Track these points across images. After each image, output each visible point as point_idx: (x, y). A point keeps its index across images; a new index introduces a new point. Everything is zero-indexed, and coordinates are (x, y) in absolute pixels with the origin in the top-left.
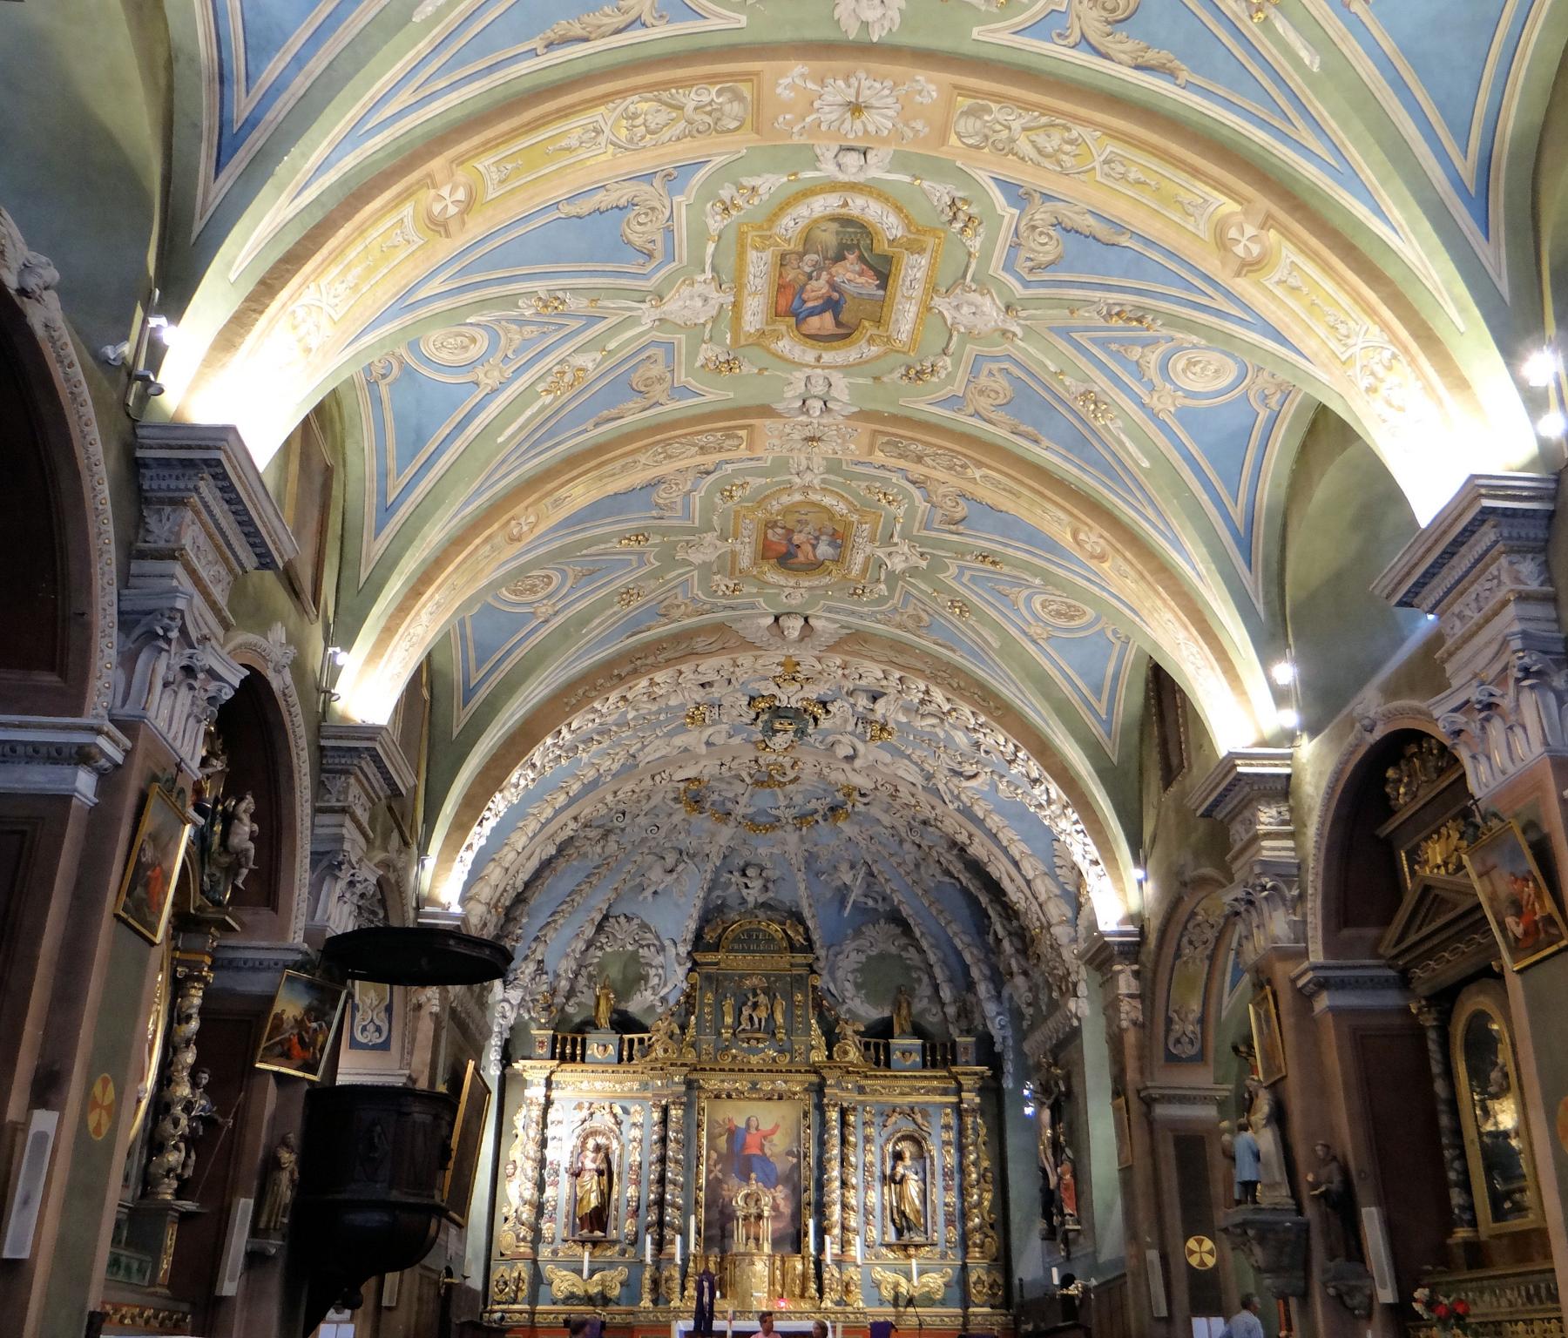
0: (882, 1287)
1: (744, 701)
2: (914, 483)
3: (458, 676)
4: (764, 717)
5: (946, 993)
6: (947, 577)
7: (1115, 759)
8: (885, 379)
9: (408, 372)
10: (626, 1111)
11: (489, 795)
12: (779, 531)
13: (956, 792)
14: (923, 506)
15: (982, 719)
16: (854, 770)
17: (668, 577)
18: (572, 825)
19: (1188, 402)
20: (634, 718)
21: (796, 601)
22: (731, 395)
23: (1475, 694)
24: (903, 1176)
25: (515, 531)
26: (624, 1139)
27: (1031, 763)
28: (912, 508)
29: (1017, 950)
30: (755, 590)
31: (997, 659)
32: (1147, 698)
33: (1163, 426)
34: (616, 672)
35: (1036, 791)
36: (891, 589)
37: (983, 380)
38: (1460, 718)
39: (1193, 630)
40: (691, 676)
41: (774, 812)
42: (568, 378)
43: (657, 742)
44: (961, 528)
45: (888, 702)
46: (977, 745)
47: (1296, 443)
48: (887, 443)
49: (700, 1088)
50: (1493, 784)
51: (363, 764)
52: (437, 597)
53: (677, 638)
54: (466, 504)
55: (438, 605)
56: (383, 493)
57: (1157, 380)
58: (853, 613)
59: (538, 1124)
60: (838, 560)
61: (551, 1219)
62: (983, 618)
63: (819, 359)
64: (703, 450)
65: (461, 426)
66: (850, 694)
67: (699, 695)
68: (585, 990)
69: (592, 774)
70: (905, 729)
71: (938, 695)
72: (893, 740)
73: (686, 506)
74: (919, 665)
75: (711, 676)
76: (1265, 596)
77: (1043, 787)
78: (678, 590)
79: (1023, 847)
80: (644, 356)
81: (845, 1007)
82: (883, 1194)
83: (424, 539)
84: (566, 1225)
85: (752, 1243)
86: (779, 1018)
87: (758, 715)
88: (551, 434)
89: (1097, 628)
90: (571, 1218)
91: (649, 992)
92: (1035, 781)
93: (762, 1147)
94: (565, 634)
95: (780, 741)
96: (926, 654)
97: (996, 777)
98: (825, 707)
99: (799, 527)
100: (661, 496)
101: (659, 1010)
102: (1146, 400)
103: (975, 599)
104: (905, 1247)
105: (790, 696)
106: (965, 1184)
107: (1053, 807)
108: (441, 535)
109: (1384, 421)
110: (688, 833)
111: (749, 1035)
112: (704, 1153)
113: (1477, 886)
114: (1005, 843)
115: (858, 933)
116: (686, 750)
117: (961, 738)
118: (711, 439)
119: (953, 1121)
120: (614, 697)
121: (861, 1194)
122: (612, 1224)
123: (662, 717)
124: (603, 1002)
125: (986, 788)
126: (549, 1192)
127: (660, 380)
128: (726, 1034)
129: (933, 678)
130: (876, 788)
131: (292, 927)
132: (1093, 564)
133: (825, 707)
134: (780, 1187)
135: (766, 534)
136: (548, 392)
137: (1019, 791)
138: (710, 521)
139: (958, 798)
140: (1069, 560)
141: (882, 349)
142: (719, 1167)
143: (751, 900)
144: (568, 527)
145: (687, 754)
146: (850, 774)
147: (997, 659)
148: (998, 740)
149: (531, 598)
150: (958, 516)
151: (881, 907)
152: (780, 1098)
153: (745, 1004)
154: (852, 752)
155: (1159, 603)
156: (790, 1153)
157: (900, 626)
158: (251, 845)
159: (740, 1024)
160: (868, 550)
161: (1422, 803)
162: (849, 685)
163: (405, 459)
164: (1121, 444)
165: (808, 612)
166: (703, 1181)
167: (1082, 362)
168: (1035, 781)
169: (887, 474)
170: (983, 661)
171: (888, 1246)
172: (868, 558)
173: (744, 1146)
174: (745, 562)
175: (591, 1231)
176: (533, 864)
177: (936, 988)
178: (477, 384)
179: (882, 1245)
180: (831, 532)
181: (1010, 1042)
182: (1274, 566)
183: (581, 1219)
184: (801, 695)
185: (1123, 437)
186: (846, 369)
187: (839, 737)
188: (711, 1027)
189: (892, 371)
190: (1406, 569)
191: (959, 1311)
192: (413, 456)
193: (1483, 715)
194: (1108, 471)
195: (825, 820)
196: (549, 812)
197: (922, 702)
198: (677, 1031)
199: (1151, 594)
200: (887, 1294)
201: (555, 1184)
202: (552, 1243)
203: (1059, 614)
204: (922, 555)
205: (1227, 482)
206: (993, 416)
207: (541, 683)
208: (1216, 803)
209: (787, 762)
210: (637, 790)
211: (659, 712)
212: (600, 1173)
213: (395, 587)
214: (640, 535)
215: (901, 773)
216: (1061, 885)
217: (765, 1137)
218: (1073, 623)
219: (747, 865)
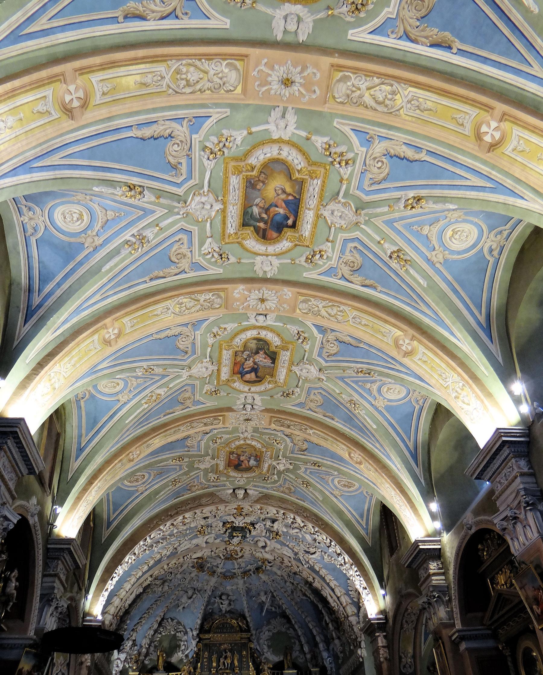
1: (221, 524)
2: (287, 436)
3: (105, 516)
4: (230, 531)
5: (306, 649)
6: (301, 472)
7: (370, 544)
8: (275, 397)
9: (92, 396)
11: (116, 567)
12: (235, 455)
13: (307, 560)
14: (290, 445)
15: (317, 529)
16: (266, 552)
17: (191, 474)
18: (150, 579)
19: (389, 403)
20: (176, 533)
21: (241, 483)
22: (216, 404)
23: (508, 513)
25: (131, 457)
27: (337, 547)
28: (286, 446)
29: (335, 628)
30: (225, 479)
31: (322, 505)
32: (381, 519)
33: (380, 412)
34: (169, 513)
35: (340, 559)
36: (279, 478)
37: (312, 397)
38: (505, 523)
39: (397, 491)
40: (200, 514)
41: (233, 571)
42: (154, 398)
43: (186, 542)
44: (305, 453)
45: (279, 523)
46: (315, 540)
47: (430, 417)
50: (521, 550)
51: (65, 555)
52: (99, 484)
53: (194, 499)
54: (112, 447)
55: (99, 488)
56: (79, 443)
57: (377, 395)
58: (264, 487)
60: (258, 466)
62: (315, 488)
63: (250, 389)
64: (205, 424)
65: (112, 417)
66: (263, 520)
67: (203, 522)
68: (153, 652)
69: (158, 556)
70: (286, 534)
71: (299, 520)
72: (281, 539)
73: (199, 446)
74: (291, 508)
75: (208, 514)
76: (424, 475)
77: (342, 557)
78: (195, 480)
79: (335, 582)
80: (183, 389)
81: (264, 657)
83: (95, 461)
87: (226, 530)
88: (147, 419)
89: (360, 491)
91: (181, 652)
92: (339, 555)
94: (149, 498)
95: (236, 540)
96: (293, 503)
97: (323, 553)
98: (253, 526)
99: (243, 454)
100: (189, 443)
101: (185, 661)
102: (373, 403)
103: (312, 480)
105: (239, 522)
107: (347, 565)
108: (102, 460)
109: (463, 409)
110: (198, 581)
111: (223, 671)
113: (520, 593)
114: (328, 581)
115: (269, 623)
116: (197, 545)
117: (308, 538)
118: (209, 420)
120: (168, 524)
123: (188, 532)
124: (160, 658)
125: (319, 558)
127: (189, 398)
129: (297, 513)
130: (275, 559)
131: (30, 628)
132: (357, 466)
133: (253, 526)
135: (230, 457)
136: (146, 403)
137: (333, 559)
138: (208, 452)
139: (308, 562)
141: (274, 385)
143: (224, 609)
145: (197, 547)
146: (264, 554)
147: (322, 505)
148: (323, 537)
149: (137, 484)
150: (304, 448)
153: (221, 657)
154: (264, 544)
155: (384, 480)
157: (282, 492)
158: (15, 592)
160: (270, 462)
161: (493, 559)
162: (263, 517)
163: (89, 430)
164: (365, 419)
167: (349, 390)
168: (339, 555)
169: (276, 433)
170: (316, 505)
172: (270, 465)
174: (221, 468)
176: (133, 596)
177: (302, 646)
178: (119, 401)
180: (255, 455)
181: (334, 670)
182: (427, 465)
184: (244, 521)
185: (366, 417)
186: (260, 393)
187: (259, 538)
188: (207, 668)
189: (277, 394)
190: (477, 465)
192: (92, 429)
193: (513, 522)
194: (361, 430)
195: (254, 573)
196: (140, 574)
197: (292, 523)
198: (192, 671)
199: (380, 477)
203: (345, 486)
204: (291, 464)
205: (405, 433)
206: (316, 410)
208: (412, 562)
209: (238, 549)
210: (177, 563)
211: (186, 530)
213: (82, 481)
214: (180, 458)
215: (285, 553)
216: (352, 599)
218: (351, 489)
219: (222, 594)
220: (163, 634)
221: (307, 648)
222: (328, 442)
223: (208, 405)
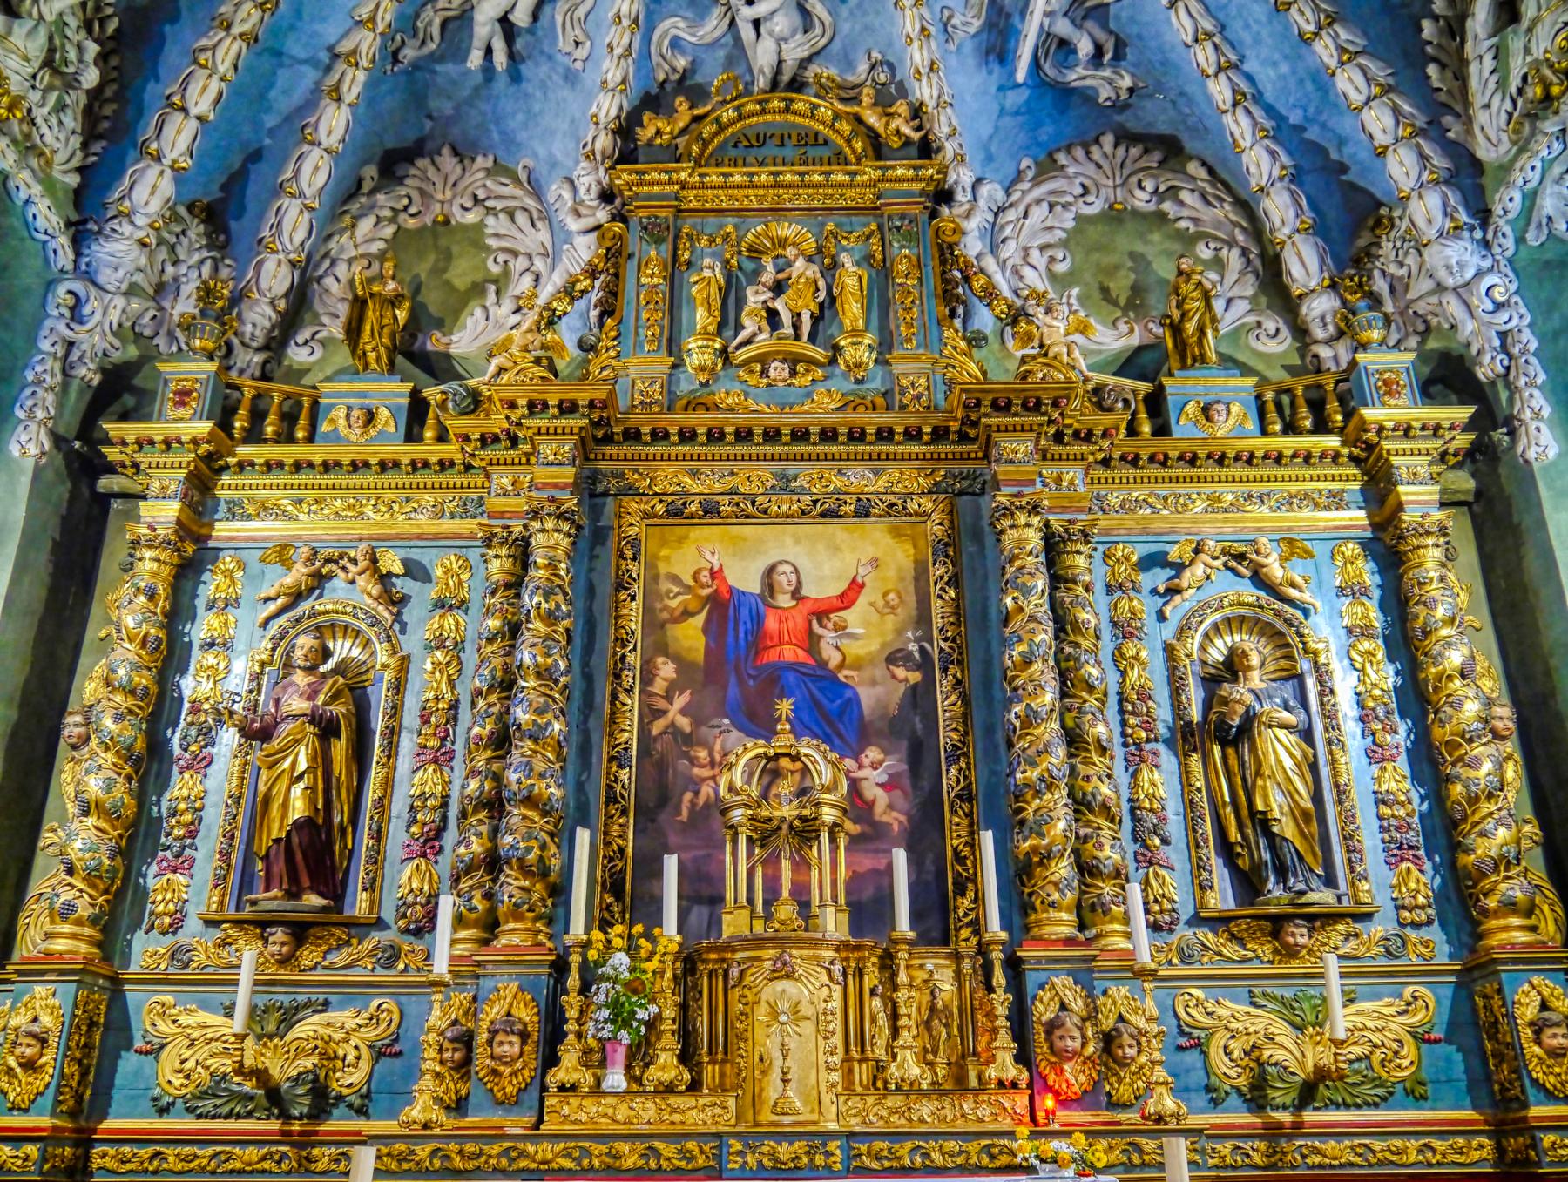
0: (1215, 1051)
10: (415, 571)
24: (1250, 718)
26: (411, 643)
49: (632, 491)
59: (152, 596)
61: (181, 863)
82: (1185, 773)
84: (220, 881)
85: (786, 911)
86: (852, 310)
90: (237, 857)
93: (811, 642)
104: (1276, 925)
106: (1439, 734)
112: (635, 659)
115: (1047, 167)
119: (1367, 573)
121: (1123, 778)
122: (360, 875)
124: (371, 315)
126: (181, 786)
128: (698, 353)
134: (873, 754)
142: (680, 701)
143: (763, 56)
151: (1108, 84)
152: (863, 512)
156: (891, 659)
159: (739, 327)
166: (629, 735)
171: (1219, 922)
173: (758, 639)
175: (293, 894)
179: (1197, 920)
183: (266, 858)
188: (655, 339)
191: (1468, 1114)
200: (1228, 1069)
201: (201, 764)
202: (175, 927)
212: (327, 729)
217: (822, 613)
220: (412, 223)
221: (1313, 262)
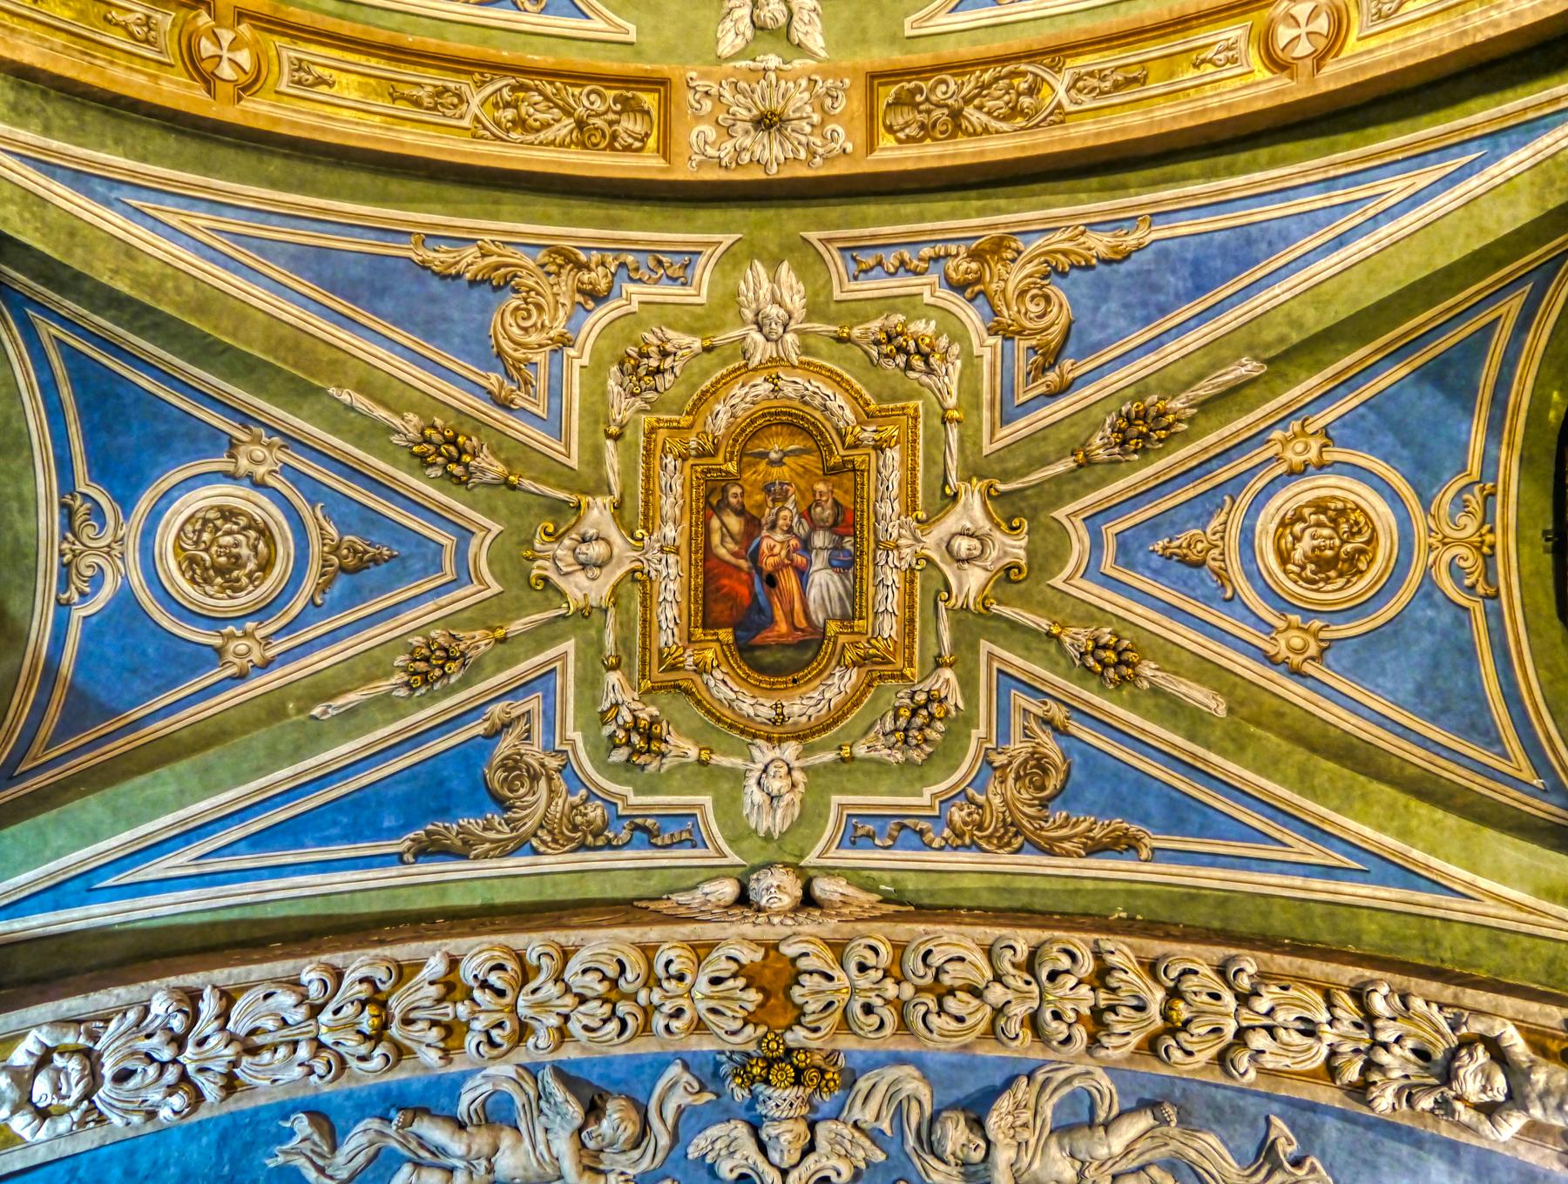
14: (987, 347)
15: (1250, 963)
27: (1417, 1003)
40: (551, 990)
48: (897, 103)
103: (1140, 614)
140: (1287, 240)
144: (319, 281)
149: (223, 603)
165: (810, 860)
170: (1204, 821)
207: (188, 835)
222: (1155, 87)
223: (598, 24)
